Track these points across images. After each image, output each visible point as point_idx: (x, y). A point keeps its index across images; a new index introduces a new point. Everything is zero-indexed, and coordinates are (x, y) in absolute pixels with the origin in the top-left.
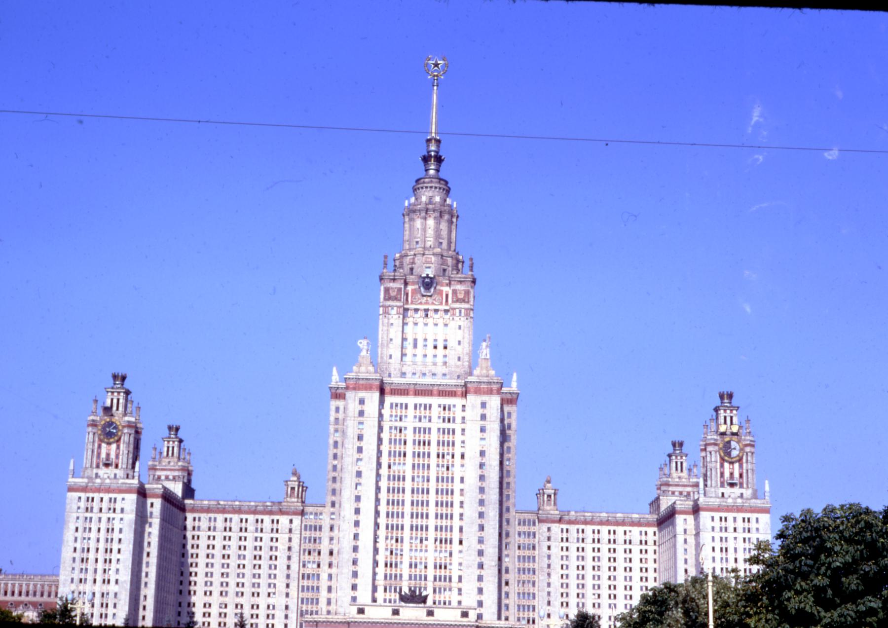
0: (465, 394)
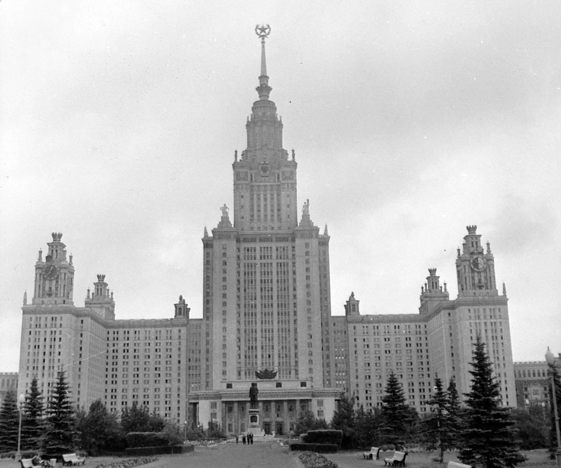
0: (293, 240)
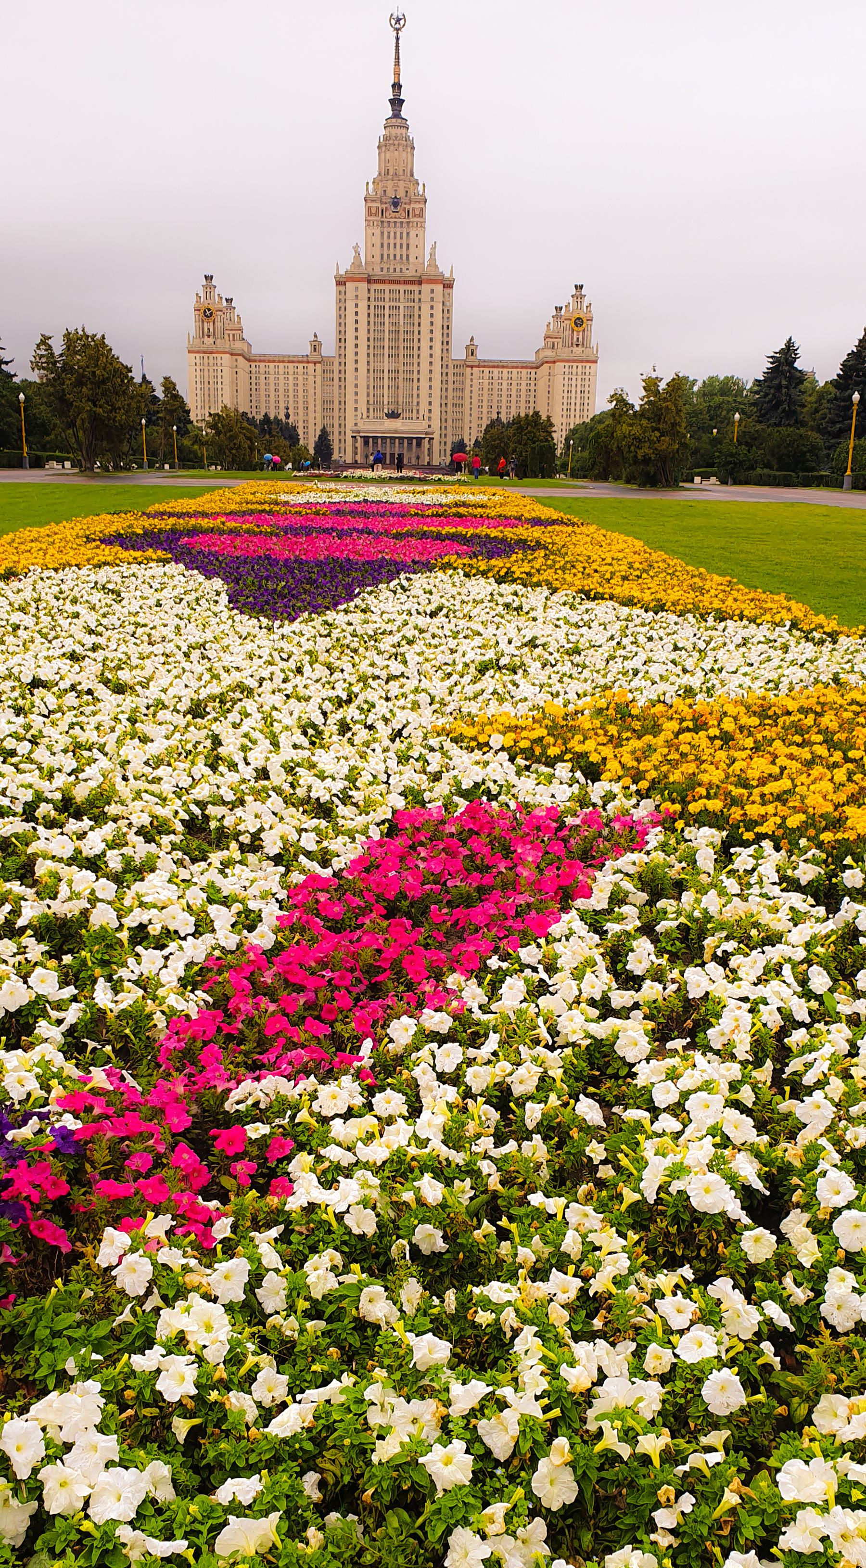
0: (420, 283)
